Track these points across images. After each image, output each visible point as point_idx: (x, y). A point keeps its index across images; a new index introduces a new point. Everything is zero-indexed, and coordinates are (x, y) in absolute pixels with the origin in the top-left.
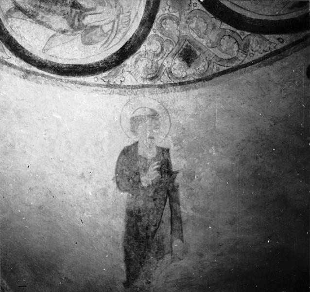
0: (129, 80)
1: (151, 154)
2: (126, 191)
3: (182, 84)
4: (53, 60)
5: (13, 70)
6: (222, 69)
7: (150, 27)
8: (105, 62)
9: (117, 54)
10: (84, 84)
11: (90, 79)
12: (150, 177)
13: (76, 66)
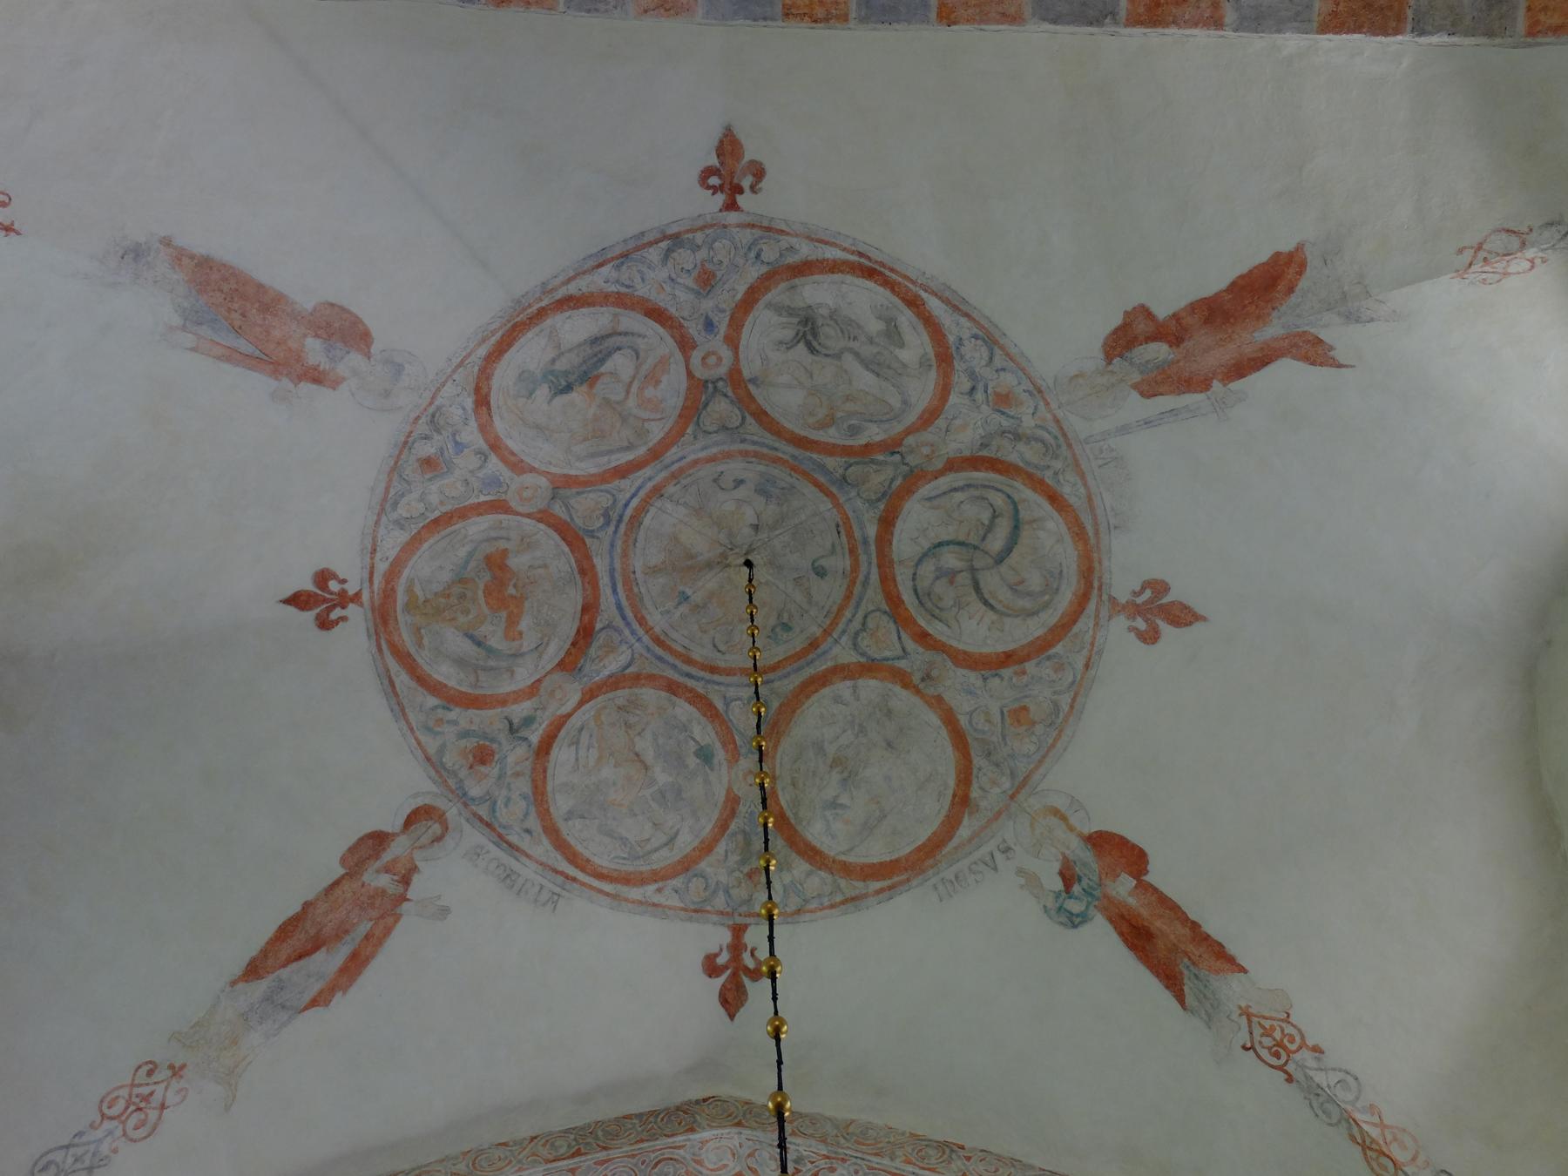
0: (449, 390)
1: (342, 369)
2: (315, 309)
3: (406, 443)
4: (536, 329)
5: (561, 279)
6: (392, 492)
7: (486, 441)
8: (488, 378)
9: (488, 395)
10: (484, 341)
11: (482, 351)
12: (314, 351)
13: (510, 345)
